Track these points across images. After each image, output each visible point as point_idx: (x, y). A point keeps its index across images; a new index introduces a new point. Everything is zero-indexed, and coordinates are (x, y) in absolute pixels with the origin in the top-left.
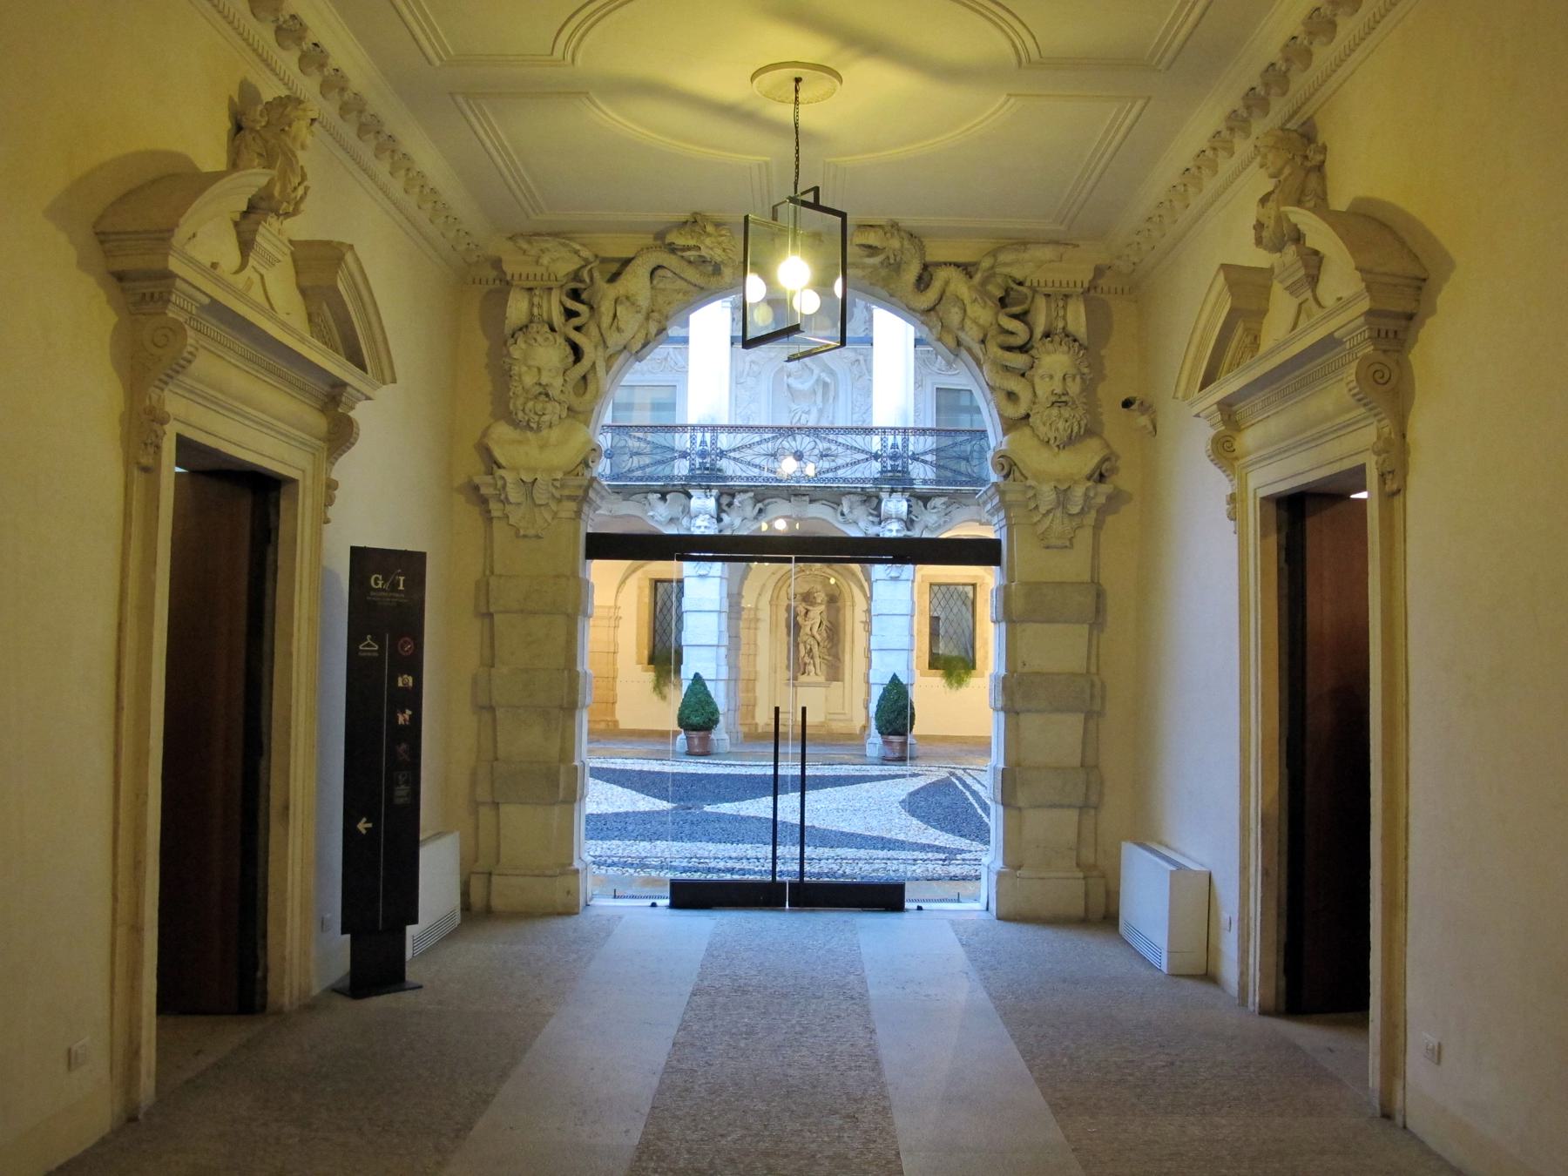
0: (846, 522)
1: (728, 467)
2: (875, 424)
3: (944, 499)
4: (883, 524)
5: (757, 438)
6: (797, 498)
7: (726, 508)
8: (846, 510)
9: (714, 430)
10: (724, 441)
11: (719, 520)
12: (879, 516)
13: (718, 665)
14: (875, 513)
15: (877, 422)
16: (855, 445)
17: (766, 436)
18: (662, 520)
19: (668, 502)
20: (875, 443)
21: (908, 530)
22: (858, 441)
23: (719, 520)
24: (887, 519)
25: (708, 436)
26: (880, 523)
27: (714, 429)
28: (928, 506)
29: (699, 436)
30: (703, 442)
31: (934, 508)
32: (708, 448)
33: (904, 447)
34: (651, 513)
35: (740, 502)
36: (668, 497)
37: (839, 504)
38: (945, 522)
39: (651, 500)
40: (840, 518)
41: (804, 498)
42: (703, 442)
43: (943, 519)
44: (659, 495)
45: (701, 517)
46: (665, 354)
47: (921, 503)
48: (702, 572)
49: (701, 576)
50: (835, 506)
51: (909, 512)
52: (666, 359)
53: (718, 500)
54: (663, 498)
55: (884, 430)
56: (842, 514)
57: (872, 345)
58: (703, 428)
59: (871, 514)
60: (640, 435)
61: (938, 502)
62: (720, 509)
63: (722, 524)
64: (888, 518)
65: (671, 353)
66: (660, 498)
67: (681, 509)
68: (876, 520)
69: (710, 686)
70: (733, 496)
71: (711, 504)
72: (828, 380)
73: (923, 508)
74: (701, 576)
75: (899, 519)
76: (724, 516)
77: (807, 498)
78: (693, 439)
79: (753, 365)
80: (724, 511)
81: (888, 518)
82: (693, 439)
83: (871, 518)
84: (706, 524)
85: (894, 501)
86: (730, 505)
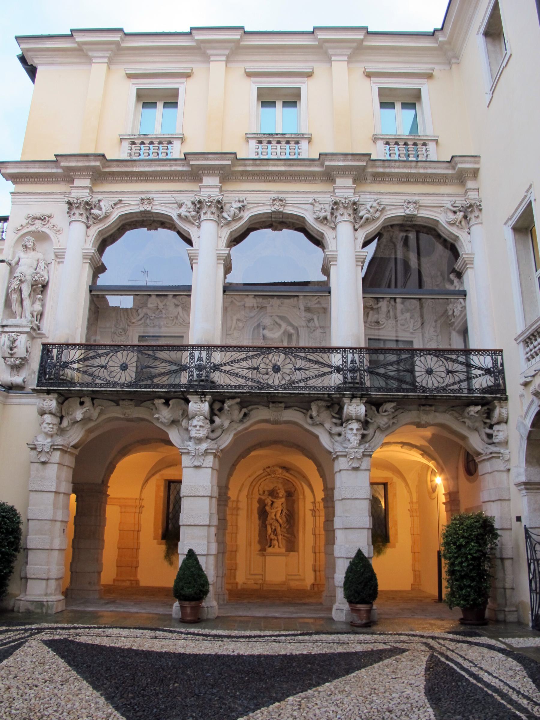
0: (314, 425)
1: (218, 377)
2: (335, 344)
3: (393, 404)
4: (344, 425)
6: (274, 405)
7: (217, 412)
8: (314, 413)
9: (209, 348)
10: (217, 357)
11: (212, 422)
12: (341, 418)
13: (208, 542)
14: (337, 416)
15: (335, 343)
16: (321, 360)
17: (251, 354)
18: (166, 421)
19: (171, 406)
20: (336, 359)
21: (364, 429)
22: (323, 357)
23: (212, 422)
24: (348, 420)
25: (204, 354)
26: (341, 425)
27: (209, 348)
28: (380, 410)
29: (197, 354)
30: (200, 359)
31: (385, 411)
32: (204, 363)
33: (361, 362)
34: (156, 416)
35: (229, 407)
36: (171, 402)
37: (309, 409)
38: (393, 423)
39: (156, 405)
40: (309, 421)
41: (280, 405)
42: (200, 359)
43: (392, 421)
44: (163, 401)
45: (197, 418)
46: (177, 313)
47: (374, 408)
48: (197, 463)
49: (196, 467)
50: (304, 411)
51: (366, 415)
52: (176, 317)
53: (211, 406)
54: (167, 404)
55: (344, 349)
56: (311, 417)
57: (330, 293)
58: (200, 347)
59: (334, 417)
61: (389, 406)
62: (212, 413)
63: (214, 425)
64: (349, 419)
65: (181, 313)
66: (164, 403)
67: (181, 412)
68: (338, 421)
69: (202, 561)
70: (223, 402)
71: (205, 407)
72: (292, 331)
73: (376, 412)
74: (196, 467)
75: (358, 420)
76: (217, 419)
77: (283, 405)
78: (192, 356)
79: (238, 322)
80: (216, 415)
81: (349, 419)
82: (192, 356)
83: (334, 420)
84: (201, 423)
85: (355, 405)
86: (221, 410)
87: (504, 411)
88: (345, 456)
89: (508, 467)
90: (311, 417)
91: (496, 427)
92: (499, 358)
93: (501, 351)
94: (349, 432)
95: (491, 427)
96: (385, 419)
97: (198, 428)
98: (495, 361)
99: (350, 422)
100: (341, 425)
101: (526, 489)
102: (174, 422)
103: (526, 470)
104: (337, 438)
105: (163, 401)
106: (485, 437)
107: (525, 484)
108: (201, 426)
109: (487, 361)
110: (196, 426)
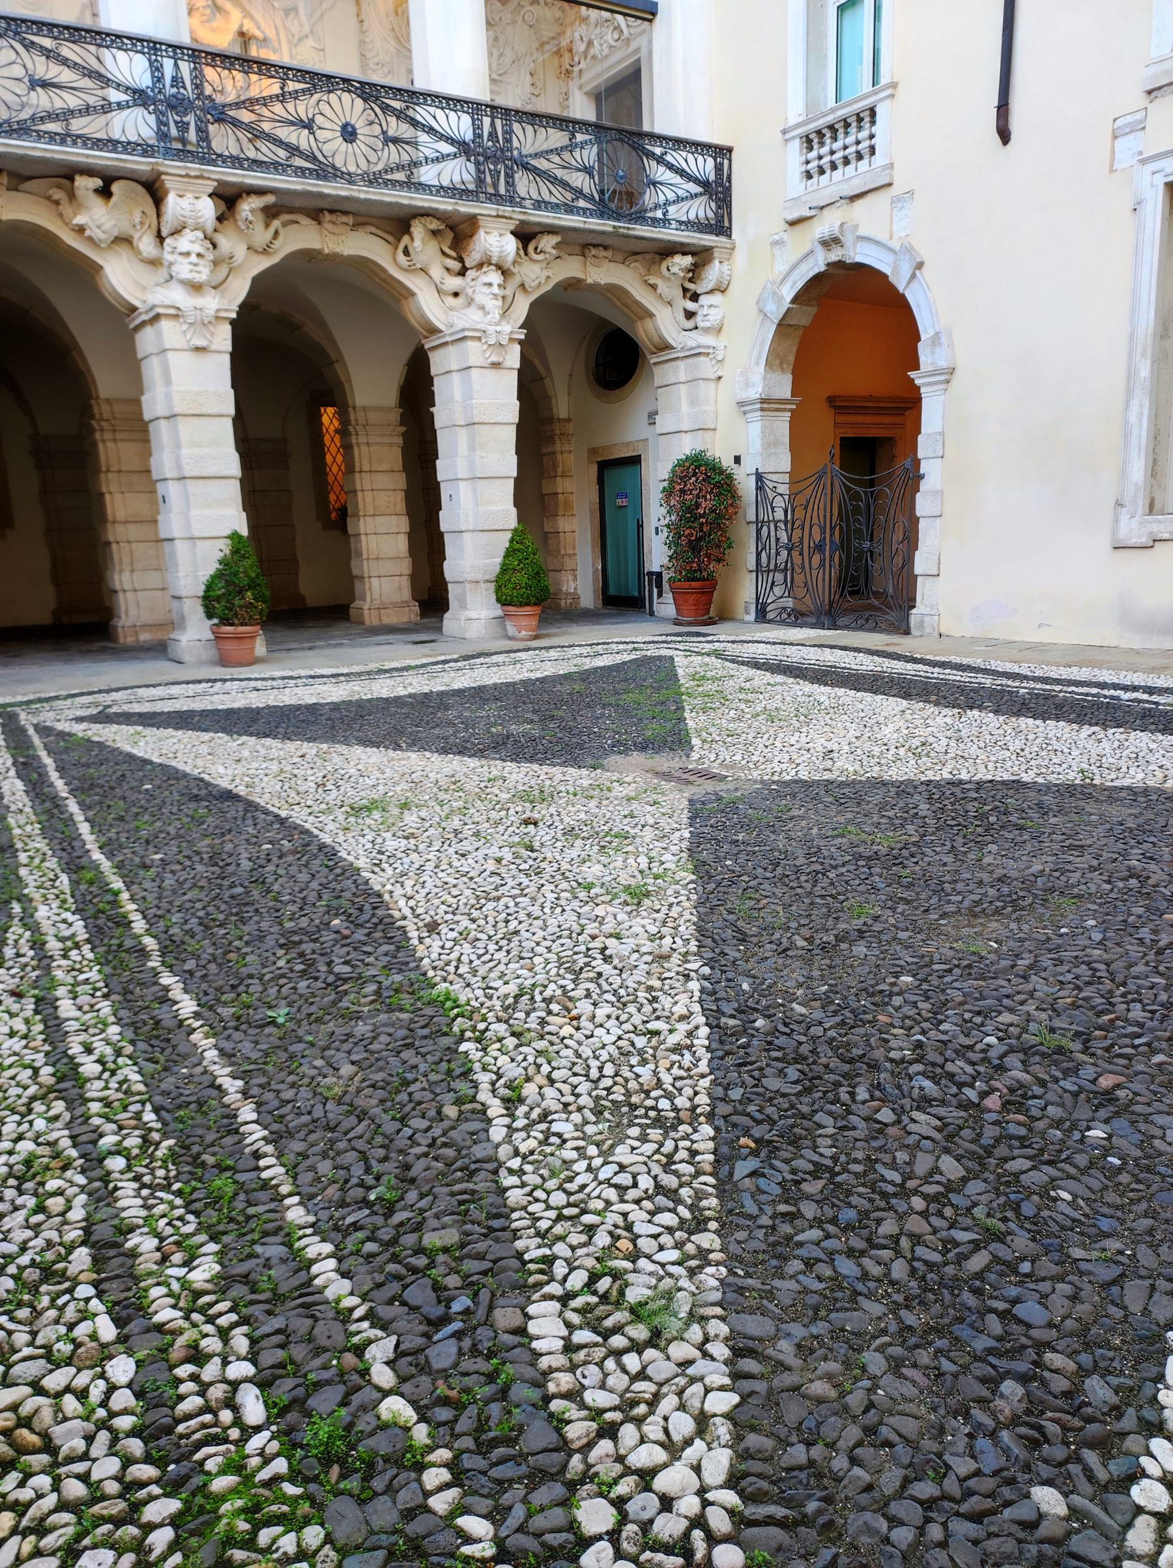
3: (555, 239)
4: (470, 274)
5: (276, 89)
6: (333, 217)
17: (292, 86)
18: (103, 236)
19: (114, 199)
26: (462, 273)
28: (531, 248)
30: (177, 81)
36: (115, 188)
40: (401, 257)
41: (344, 219)
42: (177, 81)
43: (546, 273)
48: (201, 343)
54: (105, 192)
60: (47, 43)
63: (217, 252)
66: (96, 191)
68: (455, 265)
74: (198, 349)
77: (350, 220)
85: (496, 233)
87: (725, 267)
88: (479, 339)
89: (719, 373)
90: (406, 252)
91: (703, 300)
92: (726, 162)
93: (730, 150)
94: (486, 290)
95: (695, 297)
96: (536, 268)
97: (194, 258)
98: (719, 168)
99: (485, 269)
100: (462, 273)
101: (762, 409)
102: (123, 241)
103: (765, 379)
104: (451, 301)
105: (99, 182)
106: (681, 316)
107: (763, 401)
108: (199, 255)
109: (705, 166)
110: (188, 254)
